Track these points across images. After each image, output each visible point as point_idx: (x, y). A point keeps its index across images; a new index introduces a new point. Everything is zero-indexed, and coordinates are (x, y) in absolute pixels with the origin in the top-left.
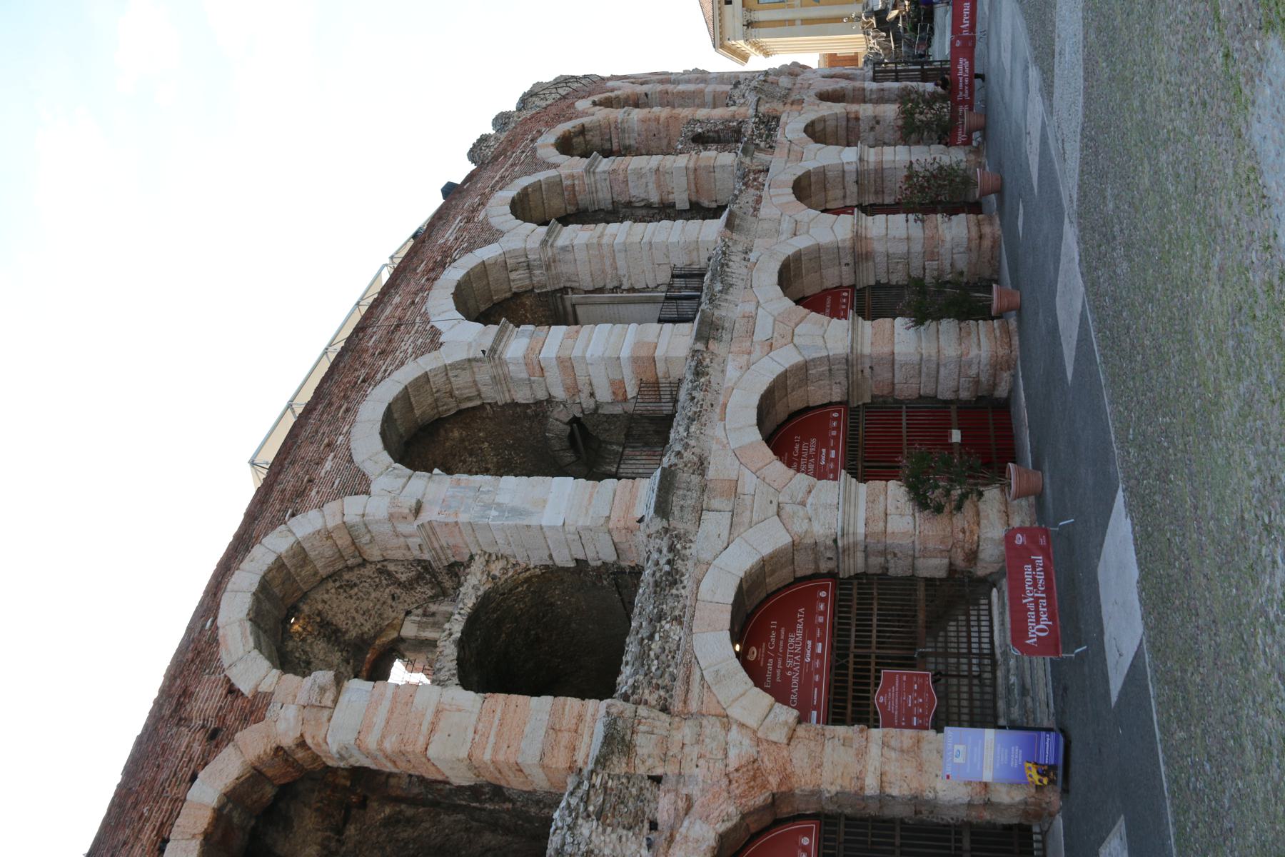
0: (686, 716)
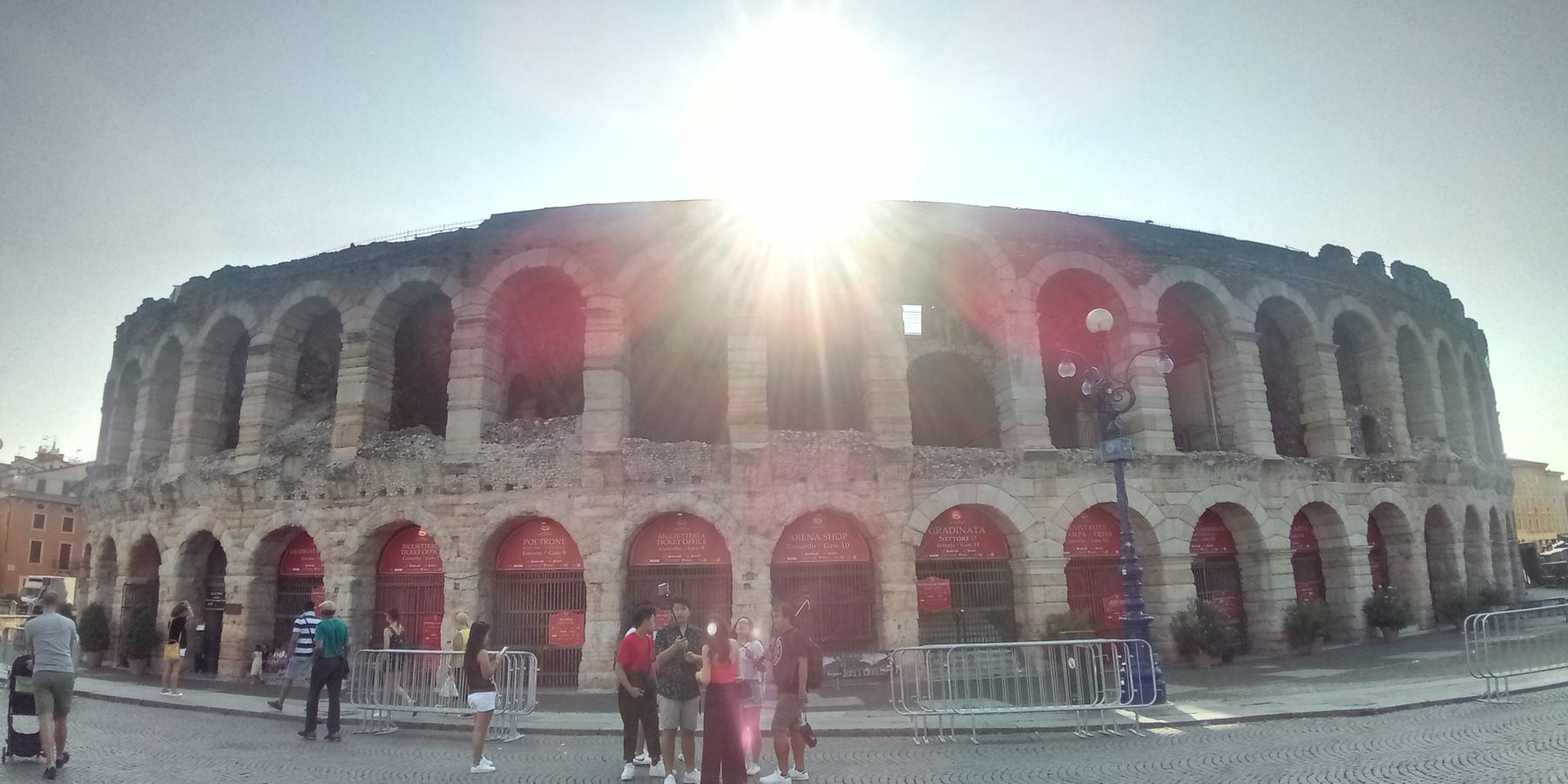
0: (911, 487)
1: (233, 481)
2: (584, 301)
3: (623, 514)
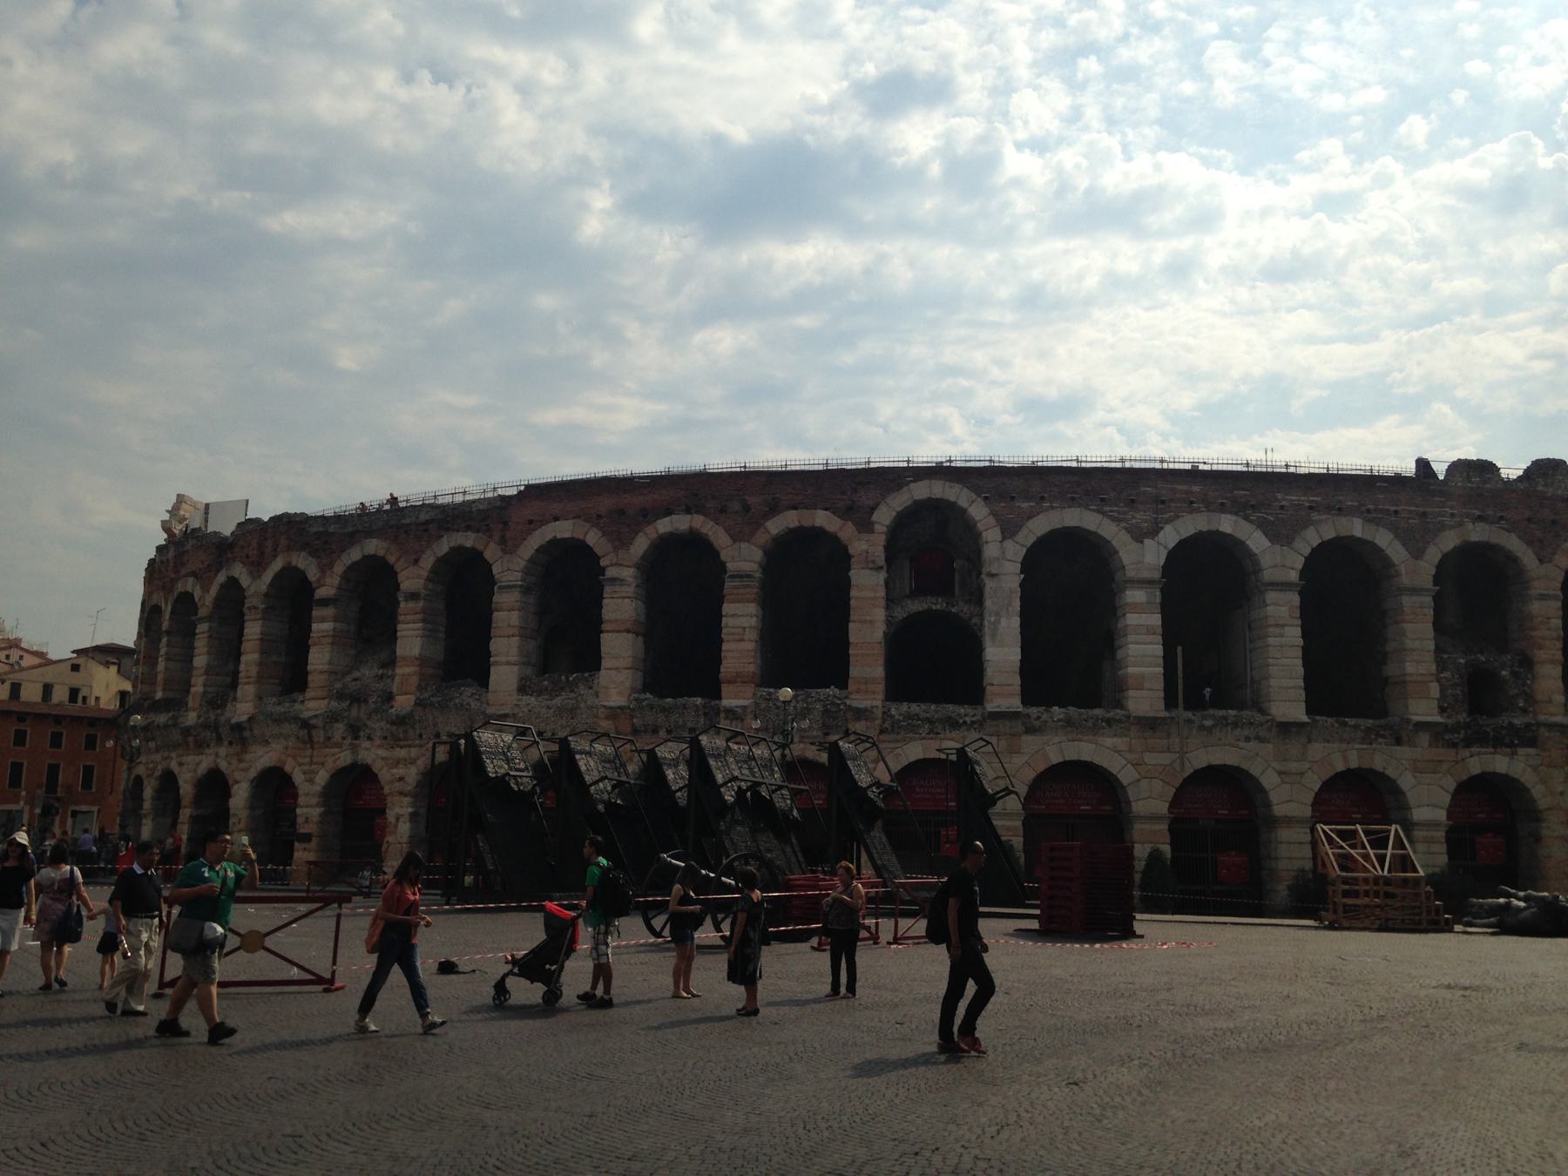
1: (306, 724)
2: (603, 570)
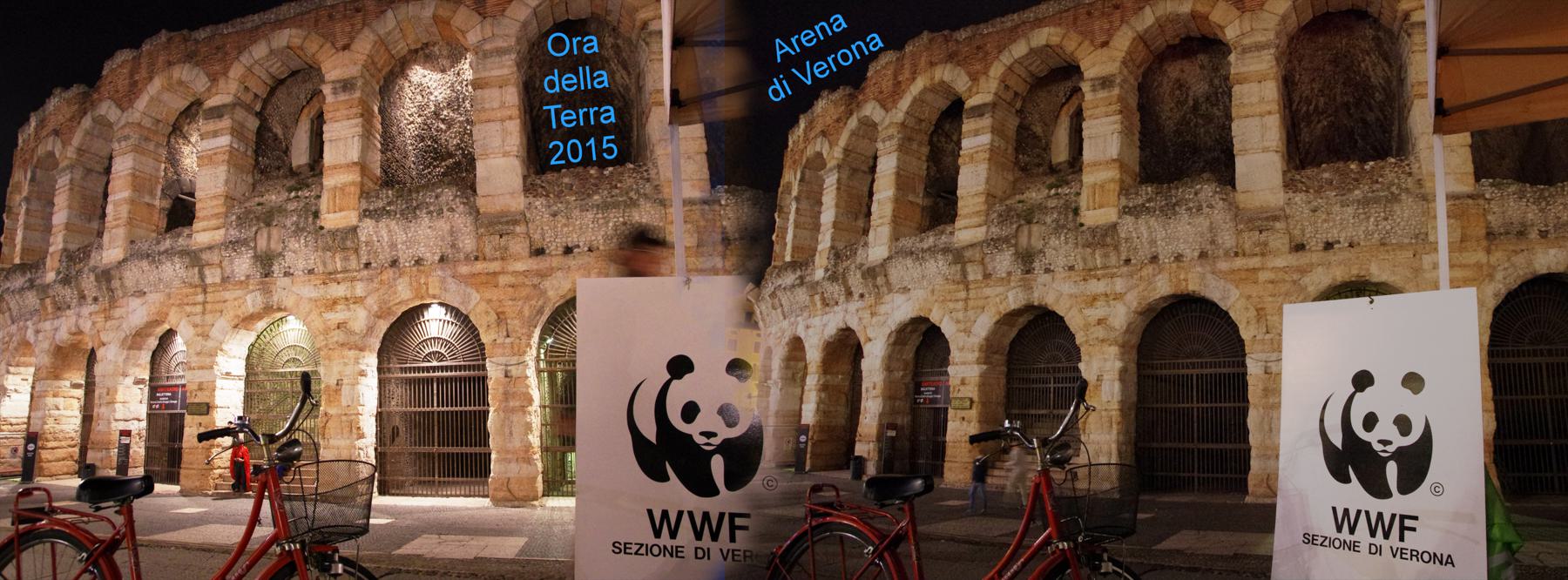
3: (1491, 277)
